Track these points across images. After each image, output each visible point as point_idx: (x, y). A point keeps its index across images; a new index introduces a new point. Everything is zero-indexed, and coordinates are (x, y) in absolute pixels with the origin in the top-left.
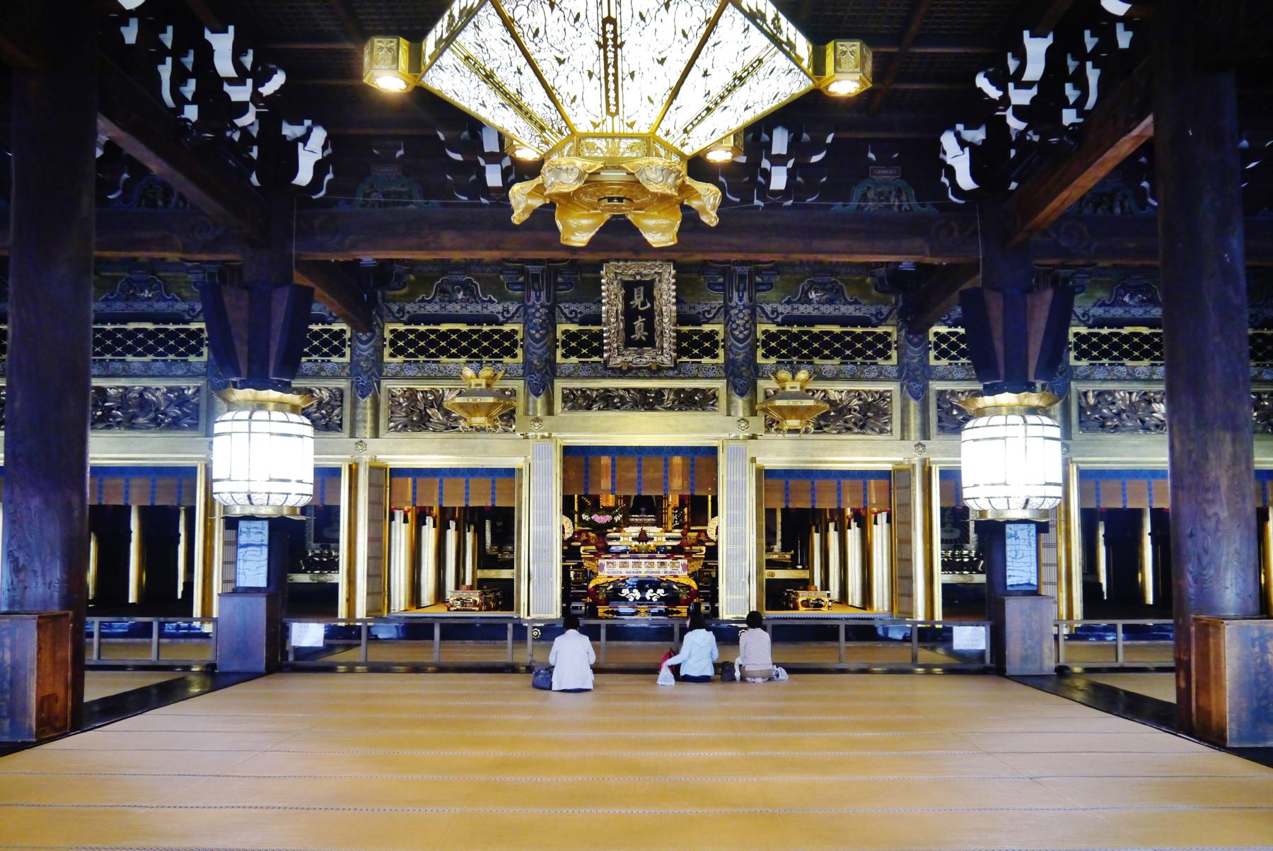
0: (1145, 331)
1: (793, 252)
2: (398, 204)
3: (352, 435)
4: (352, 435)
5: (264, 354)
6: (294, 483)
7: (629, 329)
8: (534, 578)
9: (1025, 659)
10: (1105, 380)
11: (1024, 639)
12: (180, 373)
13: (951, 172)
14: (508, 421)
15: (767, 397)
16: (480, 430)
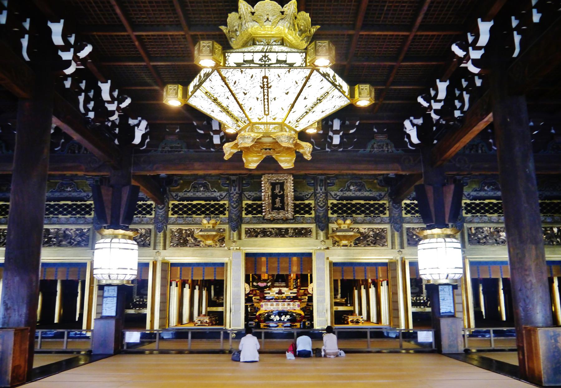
0: (495, 201)
1: (342, 170)
2: (176, 151)
3: (154, 249)
4: (154, 249)
5: (117, 214)
6: (129, 270)
7: (274, 203)
8: (233, 311)
9: (450, 346)
10: (478, 223)
11: (449, 337)
12: (82, 222)
13: (409, 136)
14: (222, 242)
15: (333, 231)
16: (210, 246)
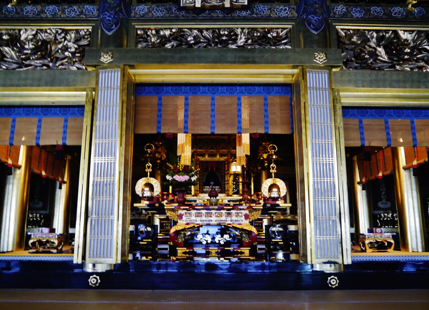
8: (93, 217)
